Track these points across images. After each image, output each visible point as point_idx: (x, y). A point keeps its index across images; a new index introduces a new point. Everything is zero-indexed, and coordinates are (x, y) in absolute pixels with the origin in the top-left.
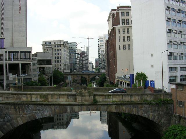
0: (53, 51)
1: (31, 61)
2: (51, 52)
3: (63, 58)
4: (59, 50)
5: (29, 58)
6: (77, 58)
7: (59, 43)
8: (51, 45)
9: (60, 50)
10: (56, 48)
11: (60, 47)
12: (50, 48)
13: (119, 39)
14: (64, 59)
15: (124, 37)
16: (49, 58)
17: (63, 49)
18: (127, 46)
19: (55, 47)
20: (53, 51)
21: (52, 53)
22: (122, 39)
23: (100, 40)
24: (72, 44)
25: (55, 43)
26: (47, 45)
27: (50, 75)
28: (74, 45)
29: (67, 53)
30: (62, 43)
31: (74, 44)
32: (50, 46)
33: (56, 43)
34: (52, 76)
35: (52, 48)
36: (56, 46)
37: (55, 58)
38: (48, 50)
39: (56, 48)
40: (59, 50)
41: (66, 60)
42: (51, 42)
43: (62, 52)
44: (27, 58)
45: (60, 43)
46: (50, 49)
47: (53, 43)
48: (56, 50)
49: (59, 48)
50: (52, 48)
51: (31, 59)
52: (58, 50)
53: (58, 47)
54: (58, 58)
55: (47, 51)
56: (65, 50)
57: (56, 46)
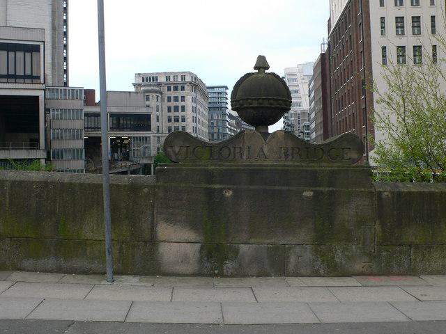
0: (163, 100)
1: (37, 86)
2: (159, 103)
3: (189, 119)
4: (180, 98)
5: (28, 73)
6: (229, 127)
7: (179, 80)
8: (159, 85)
9: (183, 98)
10: (173, 94)
11: (183, 88)
12: (156, 92)
13: (383, 27)
14: (195, 125)
15: (399, 20)
16: (143, 111)
17: (189, 95)
18: (409, 52)
19: (169, 89)
20: (163, 100)
21: (160, 107)
22: (391, 25)
23: (289, 77)
24: (216, 90)
25: (168, 78)
26: (148, 83)
27: (145, 161)
28: (221, 93)
29: (202, 110)
30: (188, 79)
31: (222, 90)
32: (157, 88)
33: (172, 80)
34: (152, 165)
35: (161, 93)
36: (172, 88)
37: (170, 120)
38: (151, 97)
39: (173, 94)
40: (180, 98)
41: (199, 126)
42: (157, 77)
43: (189, 103)
44: (20, 72)
45: (183, 78)
46: (155, 95)
47: (162, 80)
48: (172, 98)
49: (179, 94)
50: (161, 93)
51: (39, 78)
52: (176, 99)
53: (176, 89)
54: (177, 120)
55: (148, 99)
56: (195, 100)
57: (172, 88)
